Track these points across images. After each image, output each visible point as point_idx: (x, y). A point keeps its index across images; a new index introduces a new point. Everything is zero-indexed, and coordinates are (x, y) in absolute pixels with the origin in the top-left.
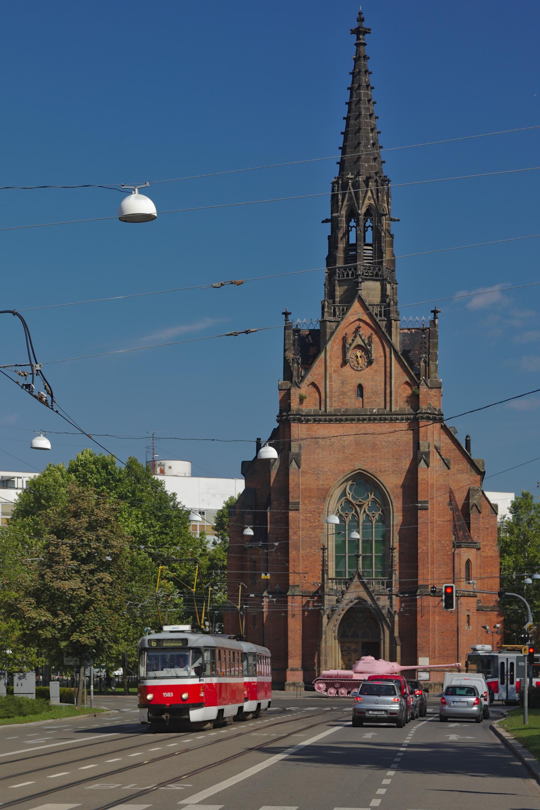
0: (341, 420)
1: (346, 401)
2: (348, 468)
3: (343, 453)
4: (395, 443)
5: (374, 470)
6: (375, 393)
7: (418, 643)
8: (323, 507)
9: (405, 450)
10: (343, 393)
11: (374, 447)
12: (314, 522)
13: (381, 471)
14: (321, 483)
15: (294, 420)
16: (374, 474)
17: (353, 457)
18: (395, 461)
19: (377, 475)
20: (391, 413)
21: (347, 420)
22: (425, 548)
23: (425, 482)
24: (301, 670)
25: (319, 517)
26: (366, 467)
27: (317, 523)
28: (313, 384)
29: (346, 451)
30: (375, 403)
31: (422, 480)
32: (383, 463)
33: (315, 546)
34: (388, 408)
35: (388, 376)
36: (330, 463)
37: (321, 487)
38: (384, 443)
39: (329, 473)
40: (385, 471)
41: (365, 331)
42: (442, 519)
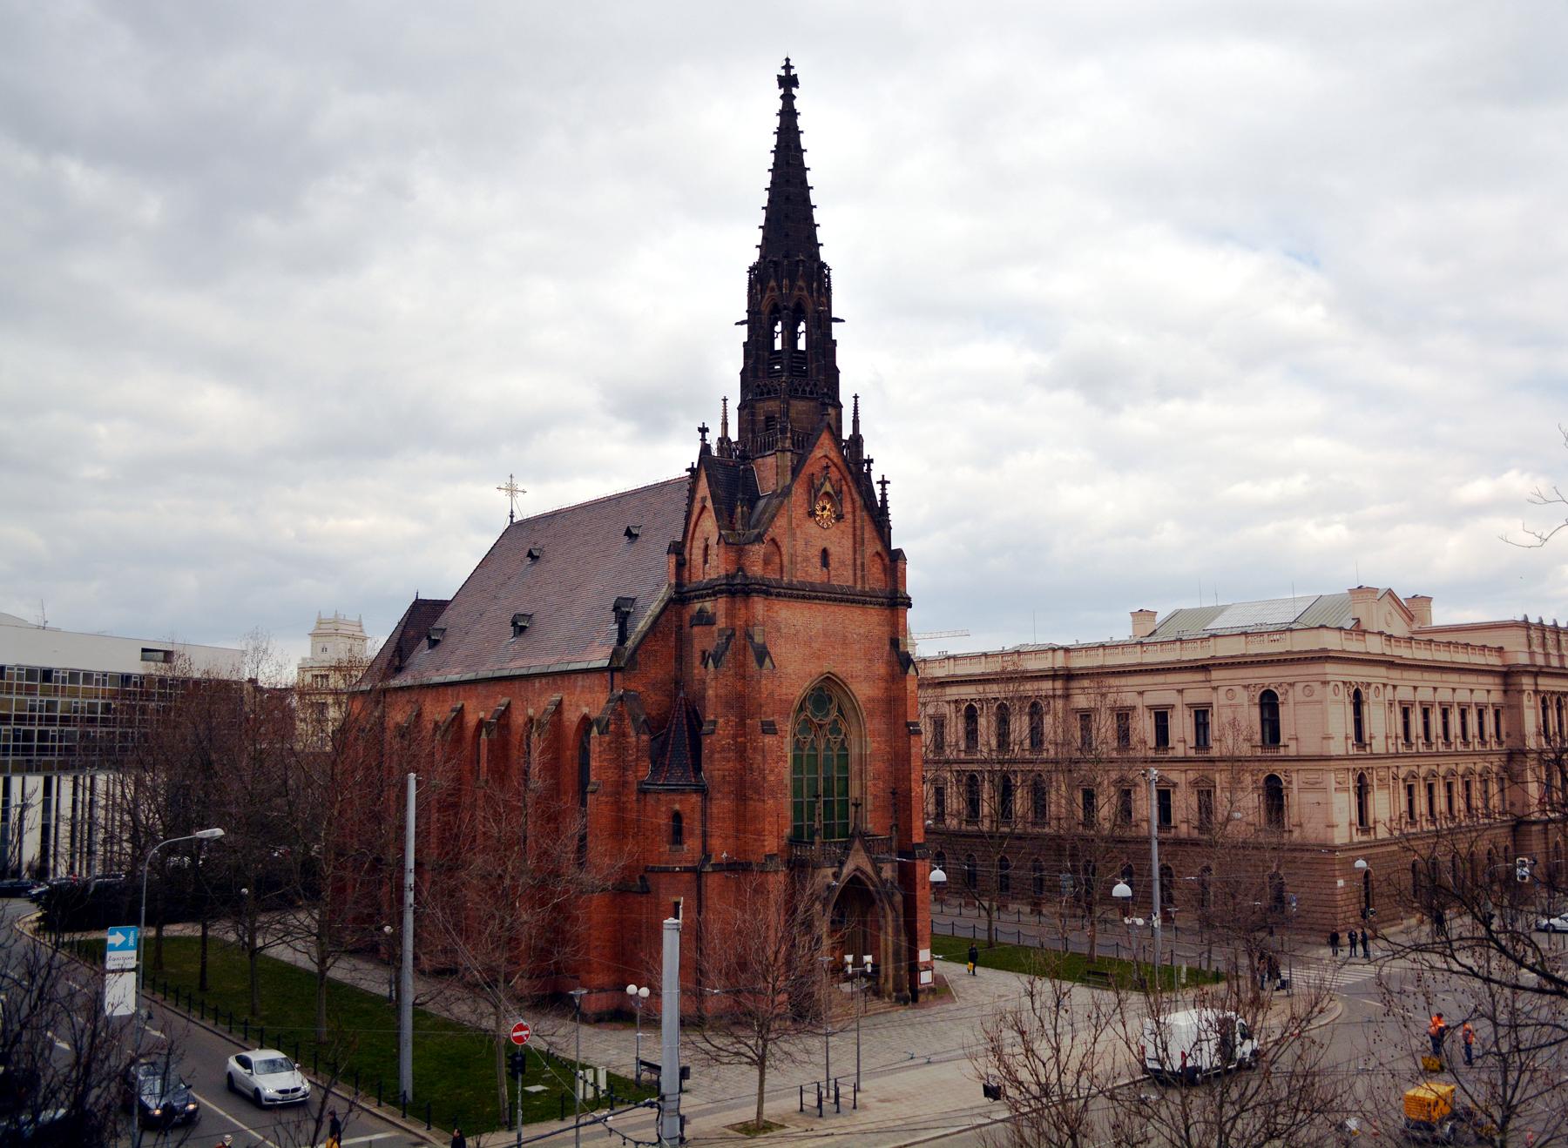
0: (810, 598)
1: (811, 571)
2: (816, 669)
6: (842, 563)
10: (807, 559)
11: (845, 642)
15: (759, 592)
20: (864, 594)
21: (816, 598)
28: (773, 540)
30: (843, 577)
34: (859, 587)
35: (858, 543)
41: (834, 474)
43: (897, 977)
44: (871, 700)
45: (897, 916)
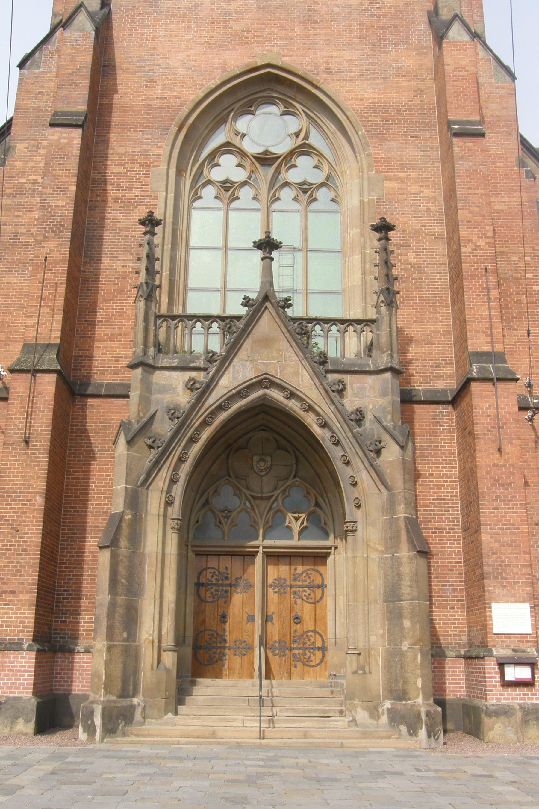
2: (236, 60)
3: (225, 27)
4: (366, 10)
5: (309, 68)
7: (485, 550)
8: (161, 152)
9: (396, 27)
12: (130, 188)
13: (328, 70)
14: (158, 92)
16: (311, 77)
17: (250, 36)
18: (368, 51)
19: (320, 79)
22: (481, 243)
23: (464, 73)
24: (30, 649)
25: (147, 175)
26: (284, 59)
27: (138, 192)
29: (231, 23)
31: (456, 69)
32: (335, 54)
33: (125, 251)
36: (187, 48)
37: (157, 103)
38: (336, 10)
39: (182, 71)
40: (340, 71)
42: (506, 199)
43: (394, 658)
44: (374, 108)
45: (390, 507)
